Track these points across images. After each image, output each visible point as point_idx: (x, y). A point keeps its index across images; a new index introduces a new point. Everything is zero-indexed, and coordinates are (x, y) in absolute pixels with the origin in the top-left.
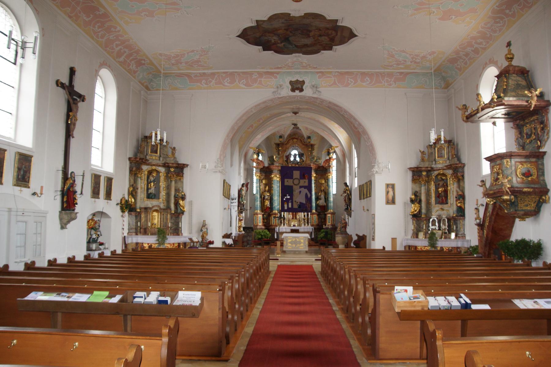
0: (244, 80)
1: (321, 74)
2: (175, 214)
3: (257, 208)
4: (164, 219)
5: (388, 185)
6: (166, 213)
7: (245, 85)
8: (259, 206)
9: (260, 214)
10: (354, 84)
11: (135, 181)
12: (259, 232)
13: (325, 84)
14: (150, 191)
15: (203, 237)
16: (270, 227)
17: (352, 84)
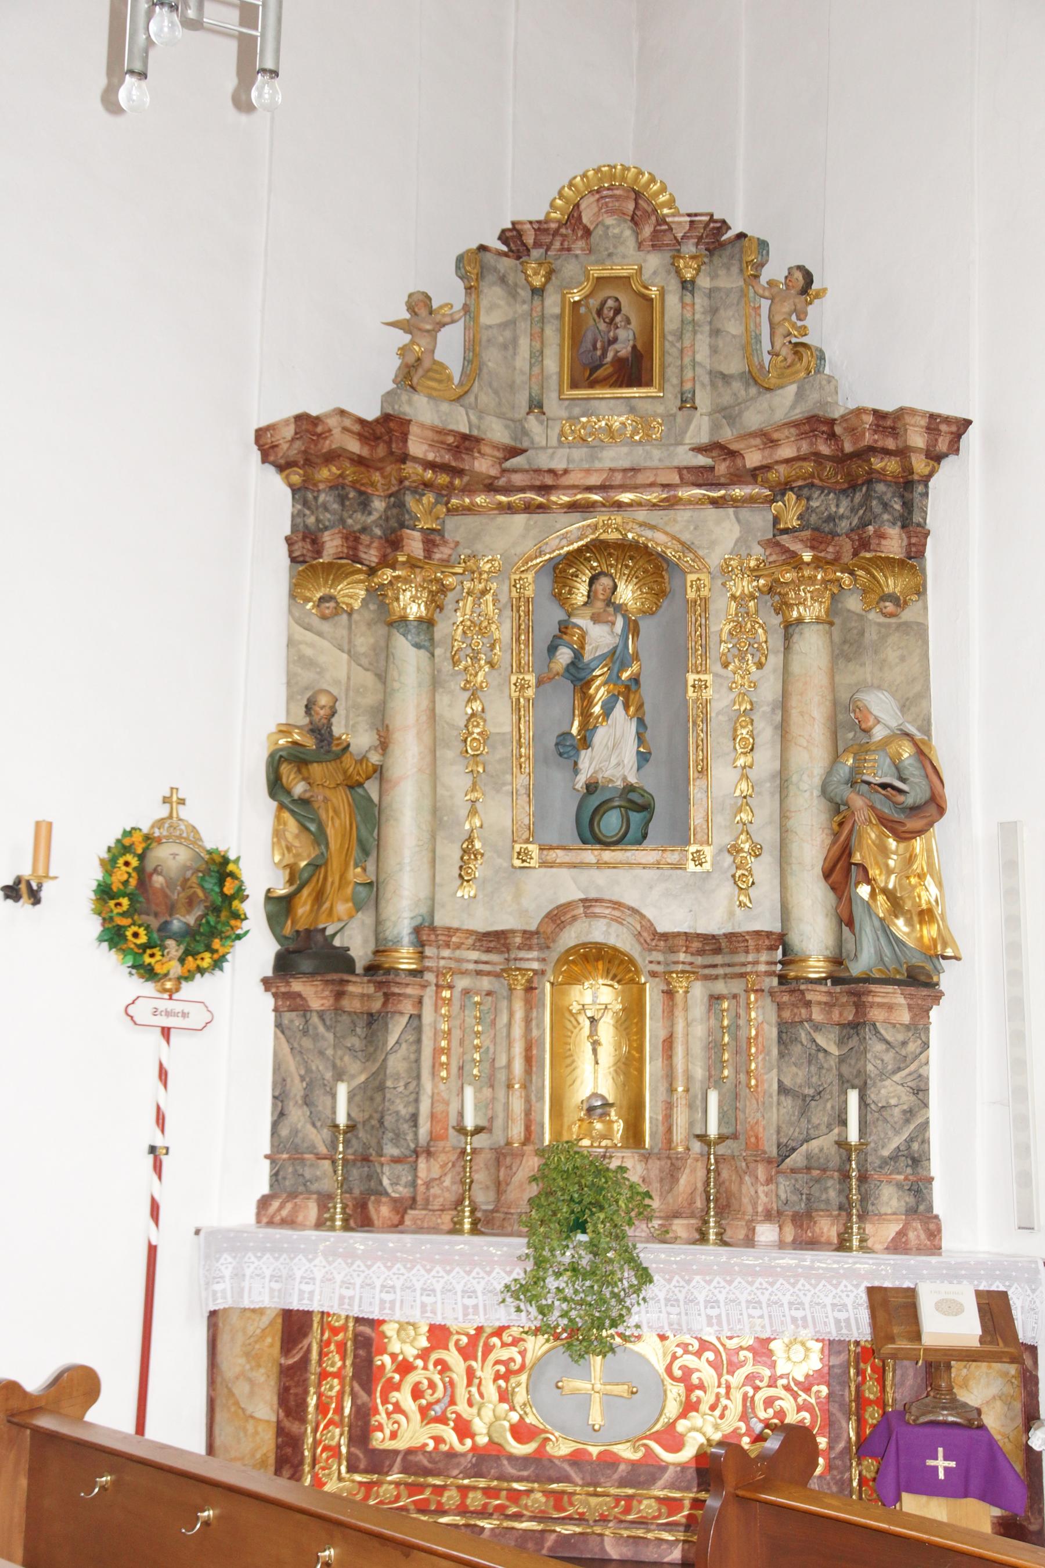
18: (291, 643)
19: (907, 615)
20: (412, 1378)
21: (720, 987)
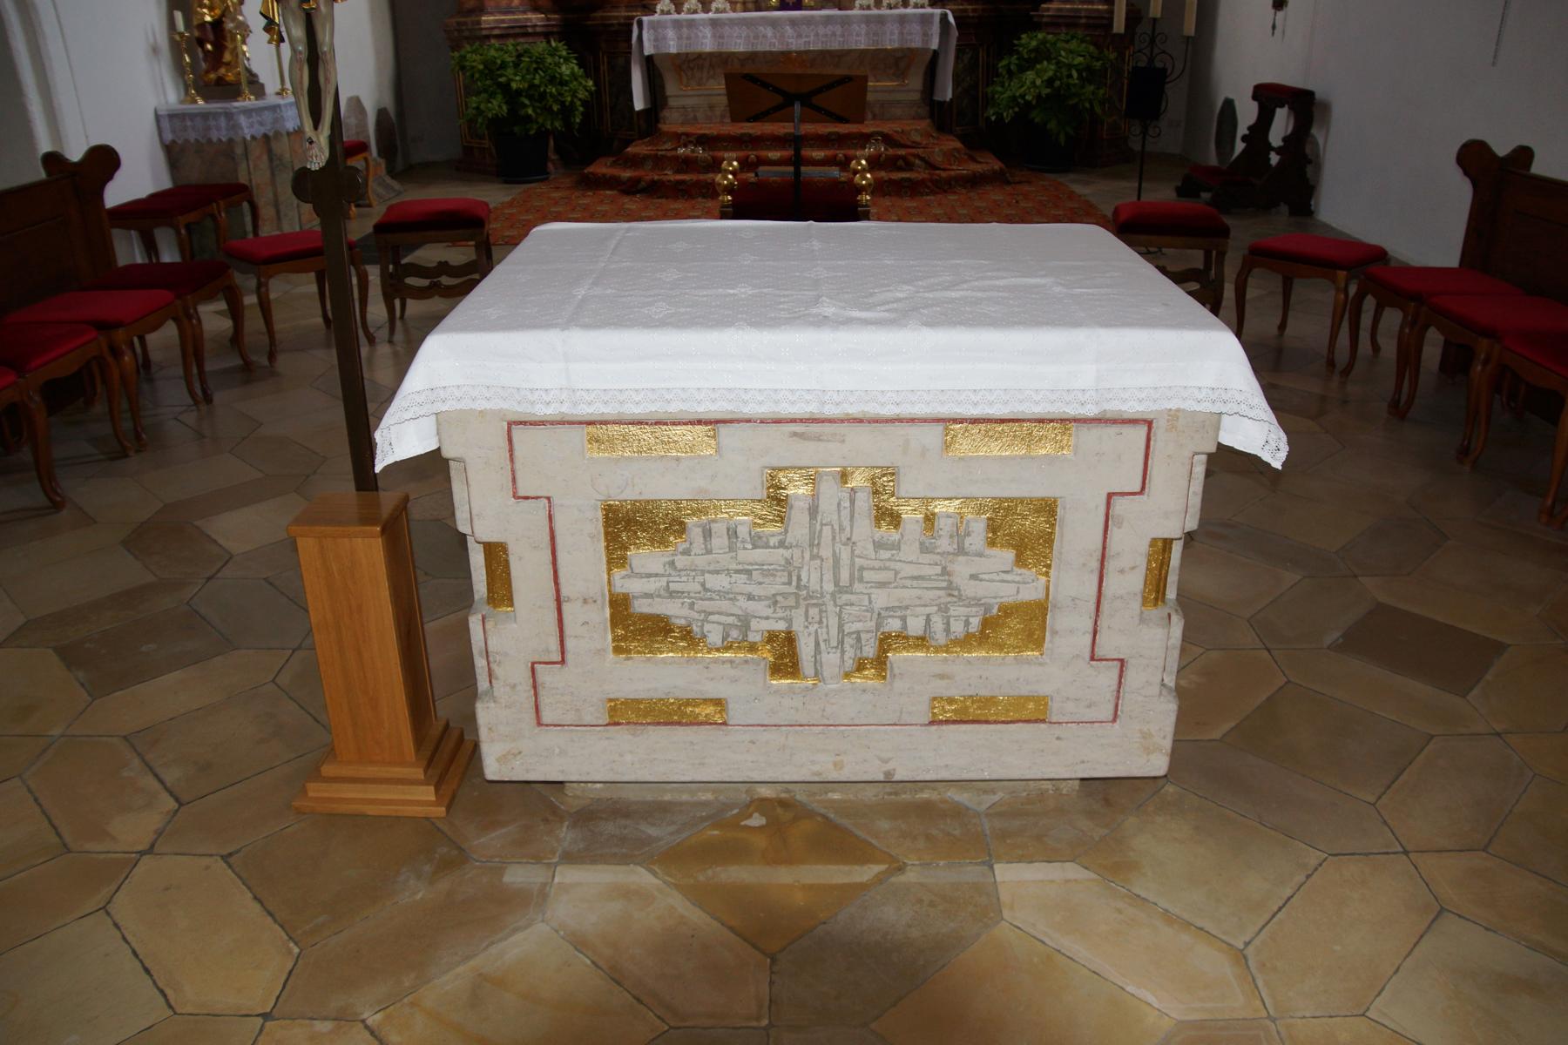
12: (492, 69)
16: (599, 14)
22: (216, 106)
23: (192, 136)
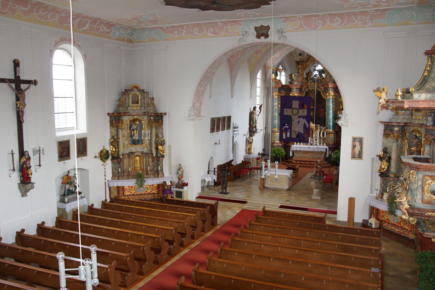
0: (211, 29)
1: (284, 18)
2: (156, 158)
3: (275, 126)
4: (146, 161)
5: (354, 139)
6: (148, 157)
7: (213, 33)
8: (276, 125)
9: (277, 132)
10: (323, 25)
11: (117, 131)
13: (291, 28)
14: (134, 138)
15: (179, 179)
17: (321, 26)
18: (110, 131)
19: (162, 127)
20: (127, 190)
21: (147, 157)
22: (249, 155)
23: (246, 157)
